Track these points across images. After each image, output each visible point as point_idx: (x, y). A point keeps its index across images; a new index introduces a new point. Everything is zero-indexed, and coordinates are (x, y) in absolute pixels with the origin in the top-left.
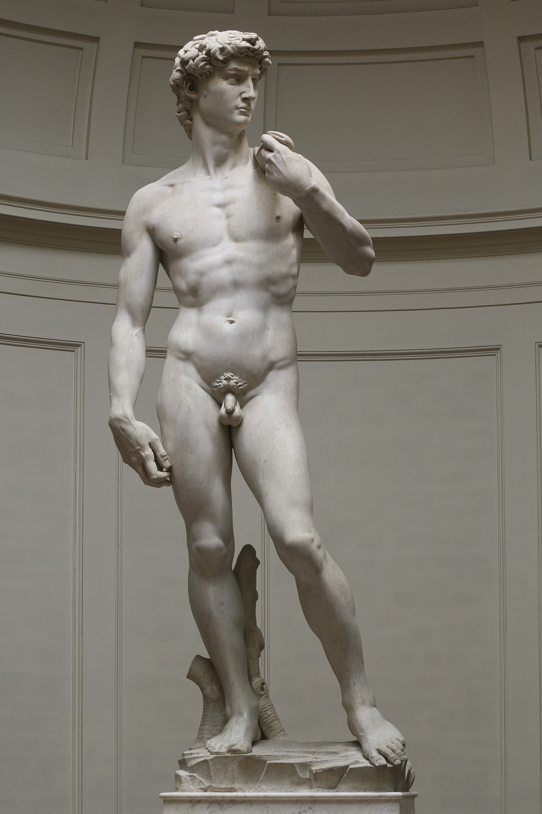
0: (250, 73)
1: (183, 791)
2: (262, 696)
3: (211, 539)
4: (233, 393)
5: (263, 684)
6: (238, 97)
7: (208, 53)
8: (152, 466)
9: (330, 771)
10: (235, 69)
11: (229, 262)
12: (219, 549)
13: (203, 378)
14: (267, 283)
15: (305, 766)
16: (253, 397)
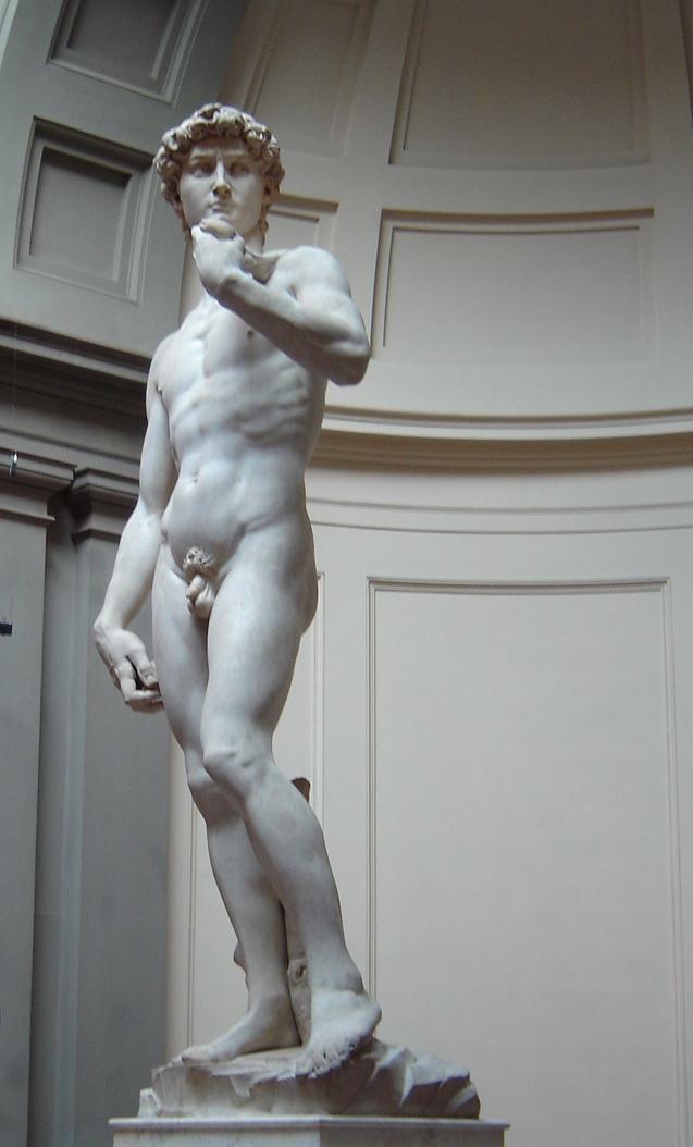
0: (219, 155)
1: (142, 1117)
2: (295, 984)
3: (201, 775)
4: (201, 574)
5: (303, 968)
6: (209, 191)
7: (167, 148)
8: (128, 684)
9: (260, 1084)
10: (196, 157)
11: (195, 405)
12: (206, 786)
13: (176, 562)
14: (235, 422)
15: (243, 1078)
16: (225, 576)
